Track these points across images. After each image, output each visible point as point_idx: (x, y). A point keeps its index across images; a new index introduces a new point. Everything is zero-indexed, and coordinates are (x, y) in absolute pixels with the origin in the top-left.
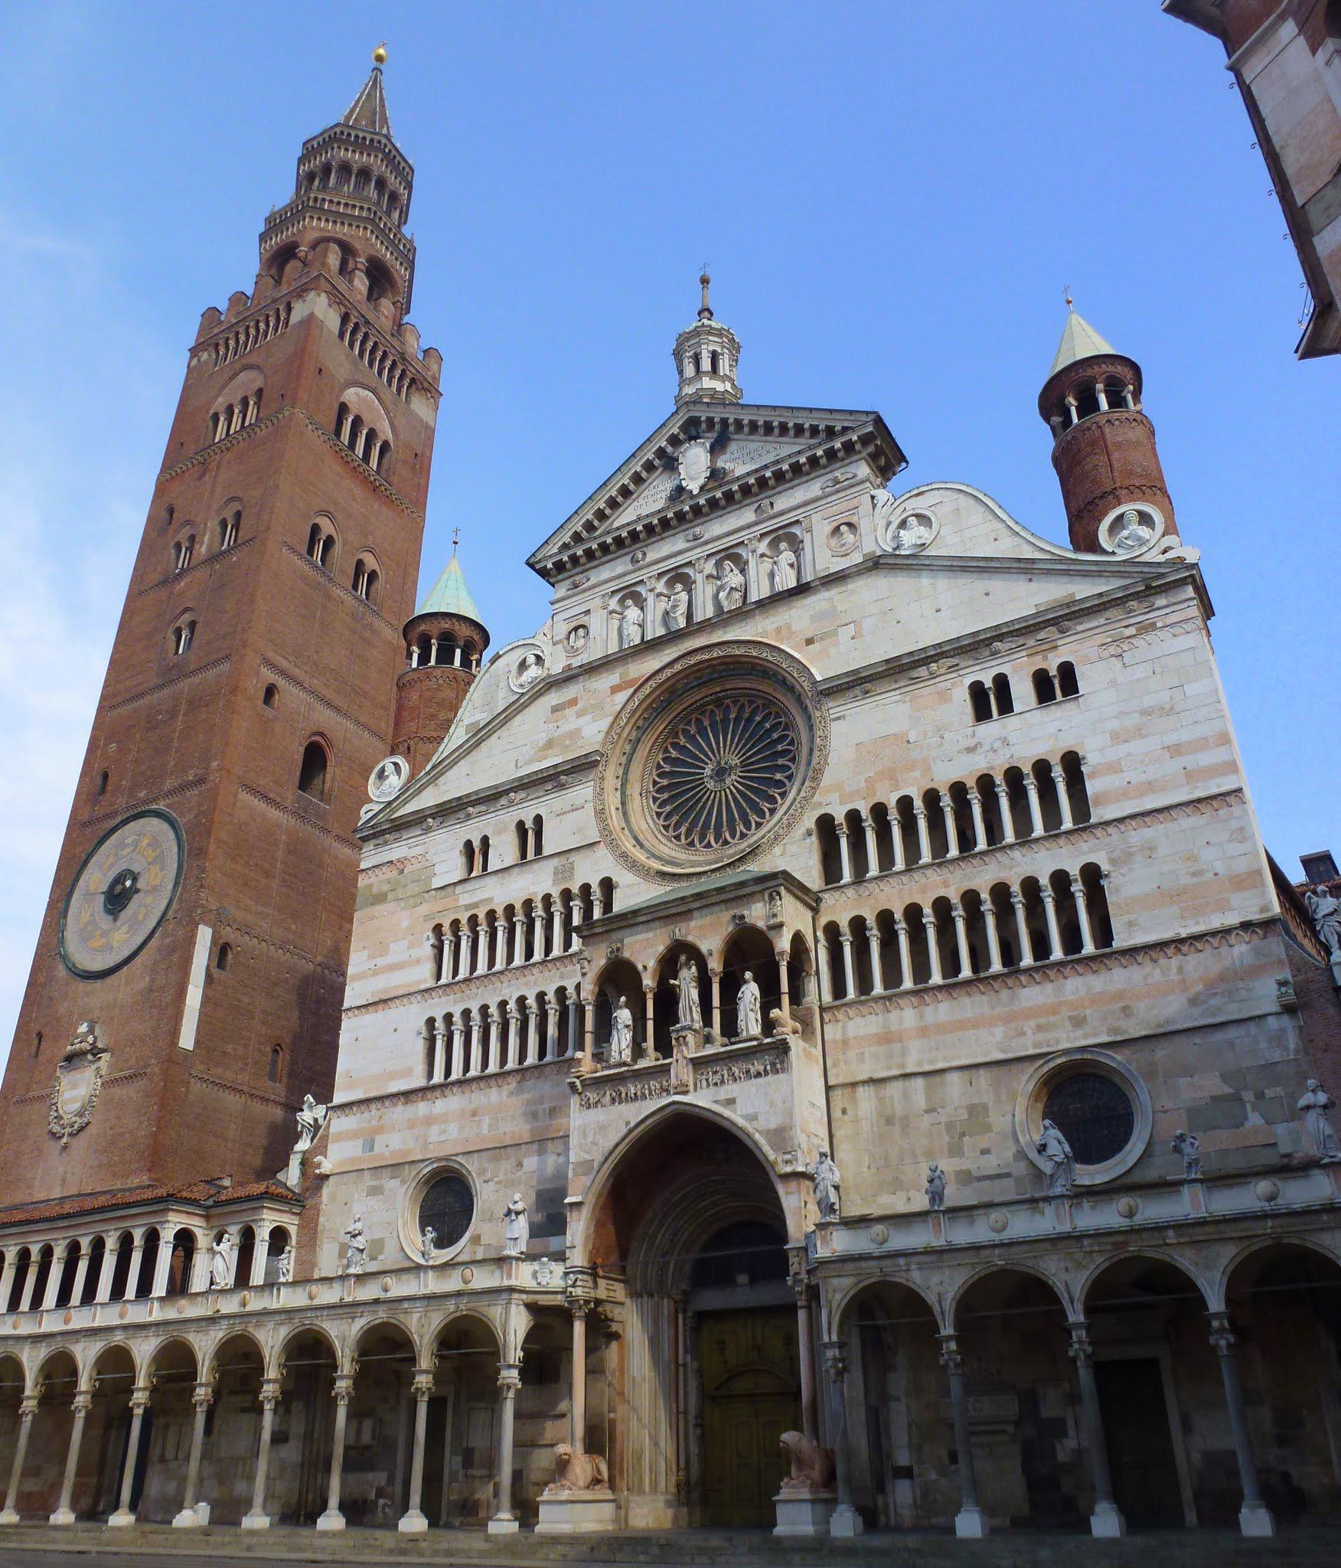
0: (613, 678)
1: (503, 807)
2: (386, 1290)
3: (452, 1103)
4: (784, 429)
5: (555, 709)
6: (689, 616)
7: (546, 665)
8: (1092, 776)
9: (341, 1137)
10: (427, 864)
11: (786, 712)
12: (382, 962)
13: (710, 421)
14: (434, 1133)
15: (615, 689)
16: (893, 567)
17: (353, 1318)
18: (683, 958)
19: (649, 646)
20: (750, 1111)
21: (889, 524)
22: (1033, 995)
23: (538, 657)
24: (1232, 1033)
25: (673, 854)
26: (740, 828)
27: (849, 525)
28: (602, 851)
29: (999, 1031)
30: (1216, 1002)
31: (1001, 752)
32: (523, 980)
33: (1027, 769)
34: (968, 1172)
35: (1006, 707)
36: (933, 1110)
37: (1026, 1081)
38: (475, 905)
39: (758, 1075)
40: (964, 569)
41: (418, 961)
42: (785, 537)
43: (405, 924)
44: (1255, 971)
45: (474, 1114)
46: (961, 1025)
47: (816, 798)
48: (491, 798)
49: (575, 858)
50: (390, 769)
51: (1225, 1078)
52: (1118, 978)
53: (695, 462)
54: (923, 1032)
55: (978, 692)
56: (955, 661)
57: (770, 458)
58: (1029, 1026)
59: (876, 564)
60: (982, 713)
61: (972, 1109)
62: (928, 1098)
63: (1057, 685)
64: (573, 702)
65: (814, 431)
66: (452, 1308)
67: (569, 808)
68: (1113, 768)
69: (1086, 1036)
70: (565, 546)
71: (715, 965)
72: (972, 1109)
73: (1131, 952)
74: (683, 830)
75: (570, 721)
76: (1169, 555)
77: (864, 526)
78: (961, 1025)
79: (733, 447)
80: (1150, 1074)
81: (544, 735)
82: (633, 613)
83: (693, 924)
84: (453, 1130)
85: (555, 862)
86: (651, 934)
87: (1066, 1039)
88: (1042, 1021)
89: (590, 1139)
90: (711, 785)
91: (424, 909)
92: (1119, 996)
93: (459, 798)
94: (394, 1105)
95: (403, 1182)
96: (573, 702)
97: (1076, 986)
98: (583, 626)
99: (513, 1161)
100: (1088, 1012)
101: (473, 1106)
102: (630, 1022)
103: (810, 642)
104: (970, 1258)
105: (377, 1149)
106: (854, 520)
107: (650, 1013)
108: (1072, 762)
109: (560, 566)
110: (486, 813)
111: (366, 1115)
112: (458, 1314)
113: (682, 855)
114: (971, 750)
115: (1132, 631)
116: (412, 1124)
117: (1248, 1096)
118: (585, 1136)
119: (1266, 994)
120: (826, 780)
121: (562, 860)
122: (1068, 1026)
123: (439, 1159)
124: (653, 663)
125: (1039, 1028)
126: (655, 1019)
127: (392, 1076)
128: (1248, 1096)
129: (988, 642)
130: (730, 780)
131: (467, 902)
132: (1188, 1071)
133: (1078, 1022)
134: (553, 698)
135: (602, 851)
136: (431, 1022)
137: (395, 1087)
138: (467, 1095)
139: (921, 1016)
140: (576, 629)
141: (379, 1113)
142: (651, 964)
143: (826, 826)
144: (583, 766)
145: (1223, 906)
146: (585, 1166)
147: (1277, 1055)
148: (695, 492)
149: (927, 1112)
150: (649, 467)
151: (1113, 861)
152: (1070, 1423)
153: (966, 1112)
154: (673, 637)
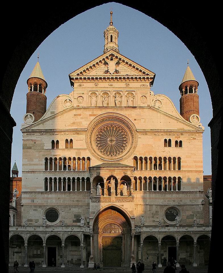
2: (35, 229)
3: (53, 196)
4: (134, 67)
5: (75, 115)
6: (108, 104)
8: (182, 162)
9: (25, 198)
12: (32, 163)
13: (117, 57)
14: (49, 201)
15: (90, 115)
21: (153, 100)
22: (168, 196)
23: (70, 100)
24: (194, 206)
25: (101, 155)
26: (115, 153)
27: (145, 96)
28: (87, 151)
30: (193, 202)
33: (172, 158)
35: (170, 145)
37: (165, 209)
41: (42, 165)
42: (131, 93)
43: (37, 155)
44: (199, 198)
45: (59, 199)
46: (156, 198)
50: (29, 116)
51: (192, 212)
52: (181, 195)
53: (112, 65)
54: (150, 198)
55: (165, 140)
56: (163, 134)
57: (129, 73)
59: (150, 107)
60: (165, 146)
62: (150, 209)
63: (179, 144)
64: (80, 115)
65: (141, 71)
68: (186, 162)
69: (175, 203)
70: (78, 75)
72: (156, 212)
73: (183, 192)
74: (103, 150)
75: (79, 119)
76: (200, 127)
77: (148, 98)
78: (156, 198)
79: (120, 65)
80: (183, 210)
81: (72, 120)
82: (94, 99)
84: (54, 201)
87: (172, 204)
88: (169, 200)
90: (109, 143)
91: (42, 153)
92: (180, 198)
93: (51, 130)
94: (39, 194)
95: (42, 209)
96: (80, 115)
97: (174, 196)
98: (81, 97)
101: (59, 197)
103: (135, 120)
104: (164, 233)
108: (179, 159)
109: (77, 79)
113: (103, 156)
116: (44, 198)
117: (195, 215)
119: (200, 201)
122: (172, 201)
123: (51, 206)
124: (99, 112)
125: (168, 201)
127: (37, 188)
128: (195, 215)
130: (114, 143)
132: (188, 210)
133: (174, 201)
134: (74, 112)
135: (87, 151)
136: (46, 179)
137: (38, 190)
139: (150, 196)
143: (135, 158)
144: (84, 131)
145: (197, 188)
146: (94, 213)
147: (199, 210)
148: (112, 74)
150: (100, 61)
151: (183, 177)
152: (164, 254)
154: (106, 107)
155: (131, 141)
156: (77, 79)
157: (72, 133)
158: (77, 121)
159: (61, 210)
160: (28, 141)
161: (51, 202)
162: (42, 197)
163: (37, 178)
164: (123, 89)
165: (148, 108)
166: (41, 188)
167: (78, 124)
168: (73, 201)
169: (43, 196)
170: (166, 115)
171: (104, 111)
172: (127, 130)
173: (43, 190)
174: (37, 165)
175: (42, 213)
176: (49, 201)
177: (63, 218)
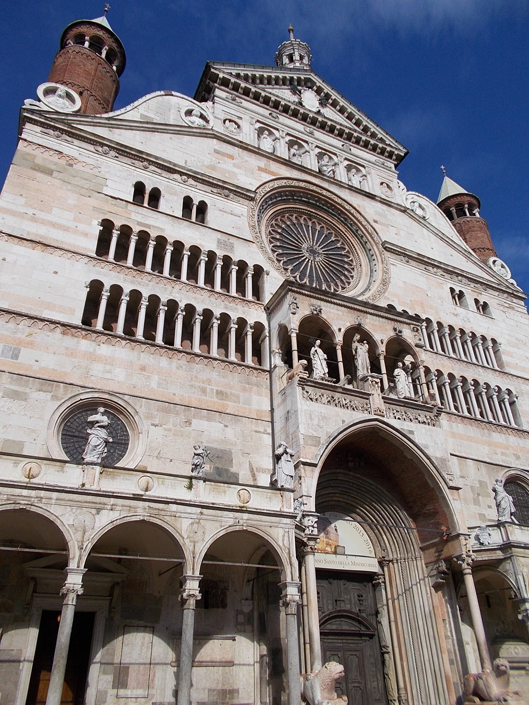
0: (263, 162)
1: (174, 180)
5: (217, 152)
7: (211, 123)
10: (98, 174)
11: (351, 246)
14: (97, 369)
15: (260, 169)
16: (412, 217)
17: (99, 510)
18: (357, 337)
19: (287, 163)
20: (424, 442)
22: (498, 437)
27: (387, 185)
29: (487, 448)
31: (467, 323)
32: (190, 294)
34: (484, 515)
36: (464, 477)
37: (502, 475)
38: (149, 226)
39: (424, 423)
40: (442, 239)
47: (386, 294)
48: (169, 169)
49: (233, 240)
54: (453, 435)
58: (499, 451)
61: (481, 482)
64: (231, 157)
66: (231, 522)
67: (230, 212)
71: (382, 349)
72: (481, 482)
74: (290, 267)
83: (367, 320)
85: (219, 235)
86: (341, 313)
88: (503, 451)
89: (315, 422)
95: (55, 398)
99: (182, 418)
100: (520, 454)
102: (325, 356)
103: (375, 222)
105: (20, 360)
106: (391, 185)
107: (340, 358)
109: (225, 83)
110: (160, 175)
111: (12, 325)
112: (237, 528)
114: (456, 315)
115: (507, 305)
116: (71, 354)
118: (311, 418)
120: (391, 288)
121: (224, 238)
126: (343, 361)
127: (50, 306)
129: (458, 275)
131: (140, 220)
133: (518, 458)
135: (254, 247)
138: (136, 353)
139: (451, 427)
140: (230, 121)
141: (28, 330)
142: (343, 330)
146: (316, 441)
149: (461, 477)
153: (477, 482)
155: (365, 268)
156: (225, 83)
157: (208, 189)
158: (223, 166)
159: (149, 416)
160: (43, 150)
161: (108, 376)
162: (67, 349)
163: (56, 273)
164: (339, 151)
165: (401, 210)
166: (72, 311)
167: (227, 175)
168: (204, 391)
169: (69, 341)
170: (442, 238)
171: (296, 174)
172: (354, 241)
173: (77, 320)
174: (66, 229)
175: (47, 418)
176: (97, 369)
177: (156, 454)
